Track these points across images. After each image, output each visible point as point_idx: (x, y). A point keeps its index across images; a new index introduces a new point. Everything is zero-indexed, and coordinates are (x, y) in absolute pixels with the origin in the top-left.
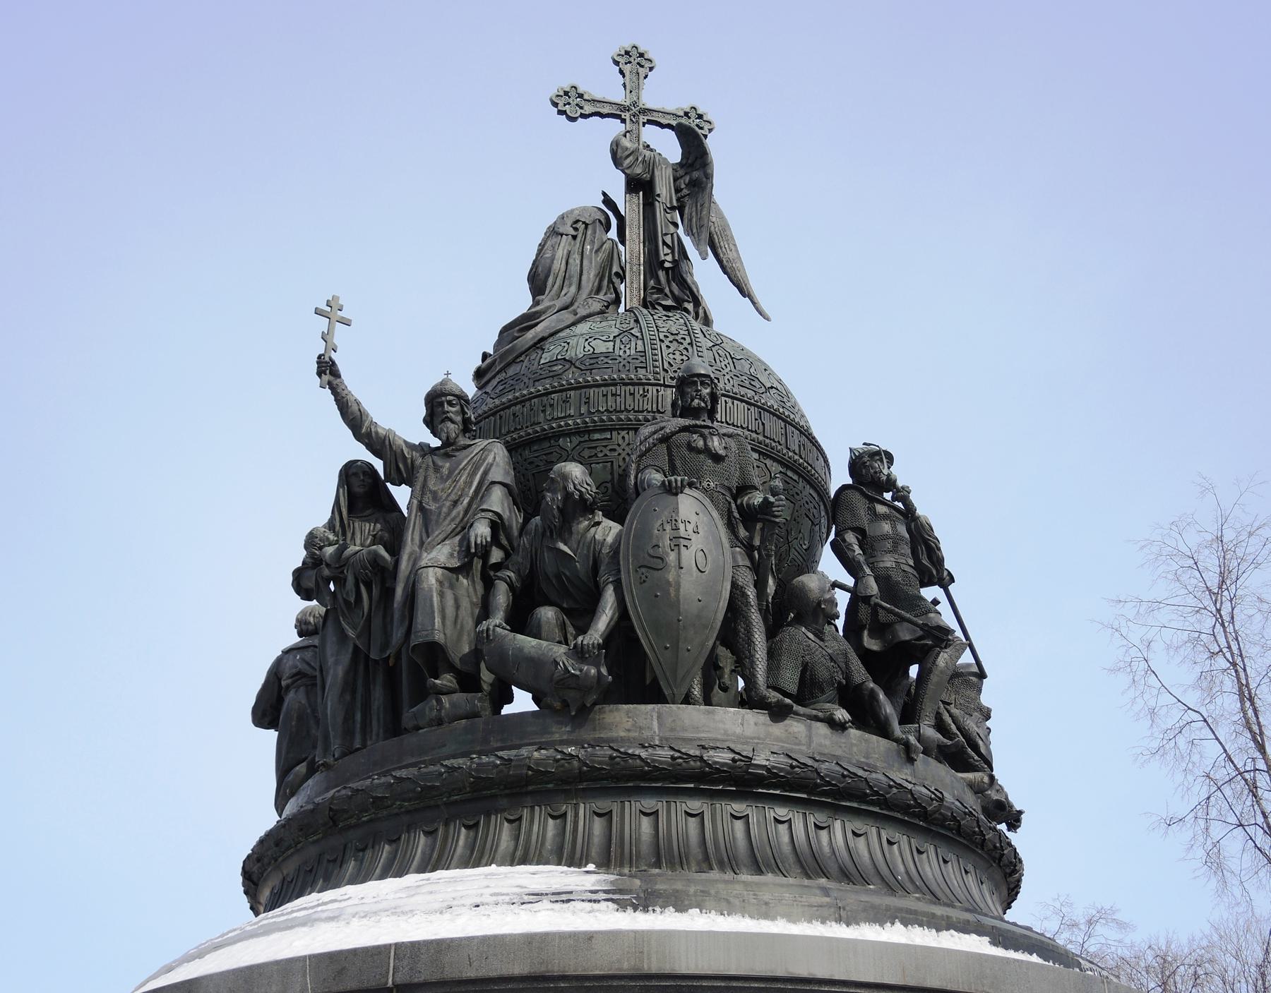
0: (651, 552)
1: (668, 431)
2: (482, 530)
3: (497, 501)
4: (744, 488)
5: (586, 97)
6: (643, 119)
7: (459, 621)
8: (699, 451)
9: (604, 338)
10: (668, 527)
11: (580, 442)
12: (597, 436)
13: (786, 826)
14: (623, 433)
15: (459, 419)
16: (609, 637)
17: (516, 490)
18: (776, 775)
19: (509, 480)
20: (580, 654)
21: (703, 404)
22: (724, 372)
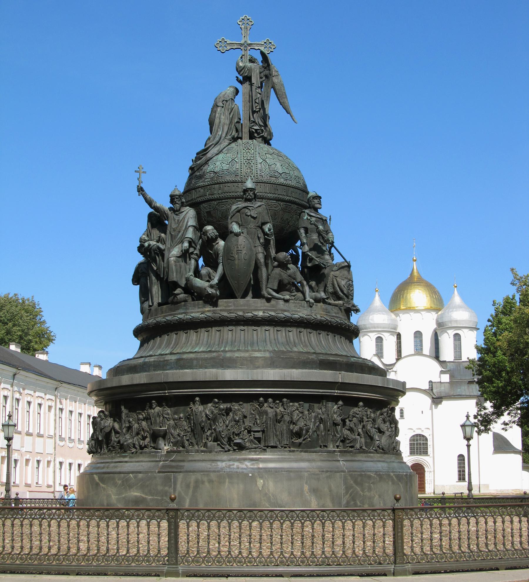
0: (231, 255)
1: (239, 208)
2: (186, 244)
3: (190, 234)
4: (264, 224)
5: (228, 43)
6: (249, 48)
7: (181, 272)
8: (248, 216)
9: (226, 163)
10: (236, 247)
11: (219, 203)
12: (224, 201)
13: (268, 331)
14: (231, 199)
15: (180, 202)
16: (220, 280)
17: (198, 226)
18: (264, 319)
19: (194, 224)
20: (212, 287)
21: (251, 198)
22: (265, 173)
